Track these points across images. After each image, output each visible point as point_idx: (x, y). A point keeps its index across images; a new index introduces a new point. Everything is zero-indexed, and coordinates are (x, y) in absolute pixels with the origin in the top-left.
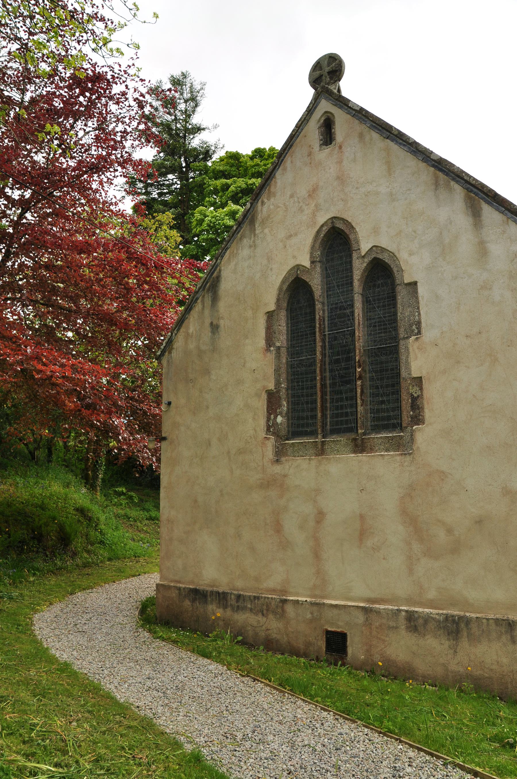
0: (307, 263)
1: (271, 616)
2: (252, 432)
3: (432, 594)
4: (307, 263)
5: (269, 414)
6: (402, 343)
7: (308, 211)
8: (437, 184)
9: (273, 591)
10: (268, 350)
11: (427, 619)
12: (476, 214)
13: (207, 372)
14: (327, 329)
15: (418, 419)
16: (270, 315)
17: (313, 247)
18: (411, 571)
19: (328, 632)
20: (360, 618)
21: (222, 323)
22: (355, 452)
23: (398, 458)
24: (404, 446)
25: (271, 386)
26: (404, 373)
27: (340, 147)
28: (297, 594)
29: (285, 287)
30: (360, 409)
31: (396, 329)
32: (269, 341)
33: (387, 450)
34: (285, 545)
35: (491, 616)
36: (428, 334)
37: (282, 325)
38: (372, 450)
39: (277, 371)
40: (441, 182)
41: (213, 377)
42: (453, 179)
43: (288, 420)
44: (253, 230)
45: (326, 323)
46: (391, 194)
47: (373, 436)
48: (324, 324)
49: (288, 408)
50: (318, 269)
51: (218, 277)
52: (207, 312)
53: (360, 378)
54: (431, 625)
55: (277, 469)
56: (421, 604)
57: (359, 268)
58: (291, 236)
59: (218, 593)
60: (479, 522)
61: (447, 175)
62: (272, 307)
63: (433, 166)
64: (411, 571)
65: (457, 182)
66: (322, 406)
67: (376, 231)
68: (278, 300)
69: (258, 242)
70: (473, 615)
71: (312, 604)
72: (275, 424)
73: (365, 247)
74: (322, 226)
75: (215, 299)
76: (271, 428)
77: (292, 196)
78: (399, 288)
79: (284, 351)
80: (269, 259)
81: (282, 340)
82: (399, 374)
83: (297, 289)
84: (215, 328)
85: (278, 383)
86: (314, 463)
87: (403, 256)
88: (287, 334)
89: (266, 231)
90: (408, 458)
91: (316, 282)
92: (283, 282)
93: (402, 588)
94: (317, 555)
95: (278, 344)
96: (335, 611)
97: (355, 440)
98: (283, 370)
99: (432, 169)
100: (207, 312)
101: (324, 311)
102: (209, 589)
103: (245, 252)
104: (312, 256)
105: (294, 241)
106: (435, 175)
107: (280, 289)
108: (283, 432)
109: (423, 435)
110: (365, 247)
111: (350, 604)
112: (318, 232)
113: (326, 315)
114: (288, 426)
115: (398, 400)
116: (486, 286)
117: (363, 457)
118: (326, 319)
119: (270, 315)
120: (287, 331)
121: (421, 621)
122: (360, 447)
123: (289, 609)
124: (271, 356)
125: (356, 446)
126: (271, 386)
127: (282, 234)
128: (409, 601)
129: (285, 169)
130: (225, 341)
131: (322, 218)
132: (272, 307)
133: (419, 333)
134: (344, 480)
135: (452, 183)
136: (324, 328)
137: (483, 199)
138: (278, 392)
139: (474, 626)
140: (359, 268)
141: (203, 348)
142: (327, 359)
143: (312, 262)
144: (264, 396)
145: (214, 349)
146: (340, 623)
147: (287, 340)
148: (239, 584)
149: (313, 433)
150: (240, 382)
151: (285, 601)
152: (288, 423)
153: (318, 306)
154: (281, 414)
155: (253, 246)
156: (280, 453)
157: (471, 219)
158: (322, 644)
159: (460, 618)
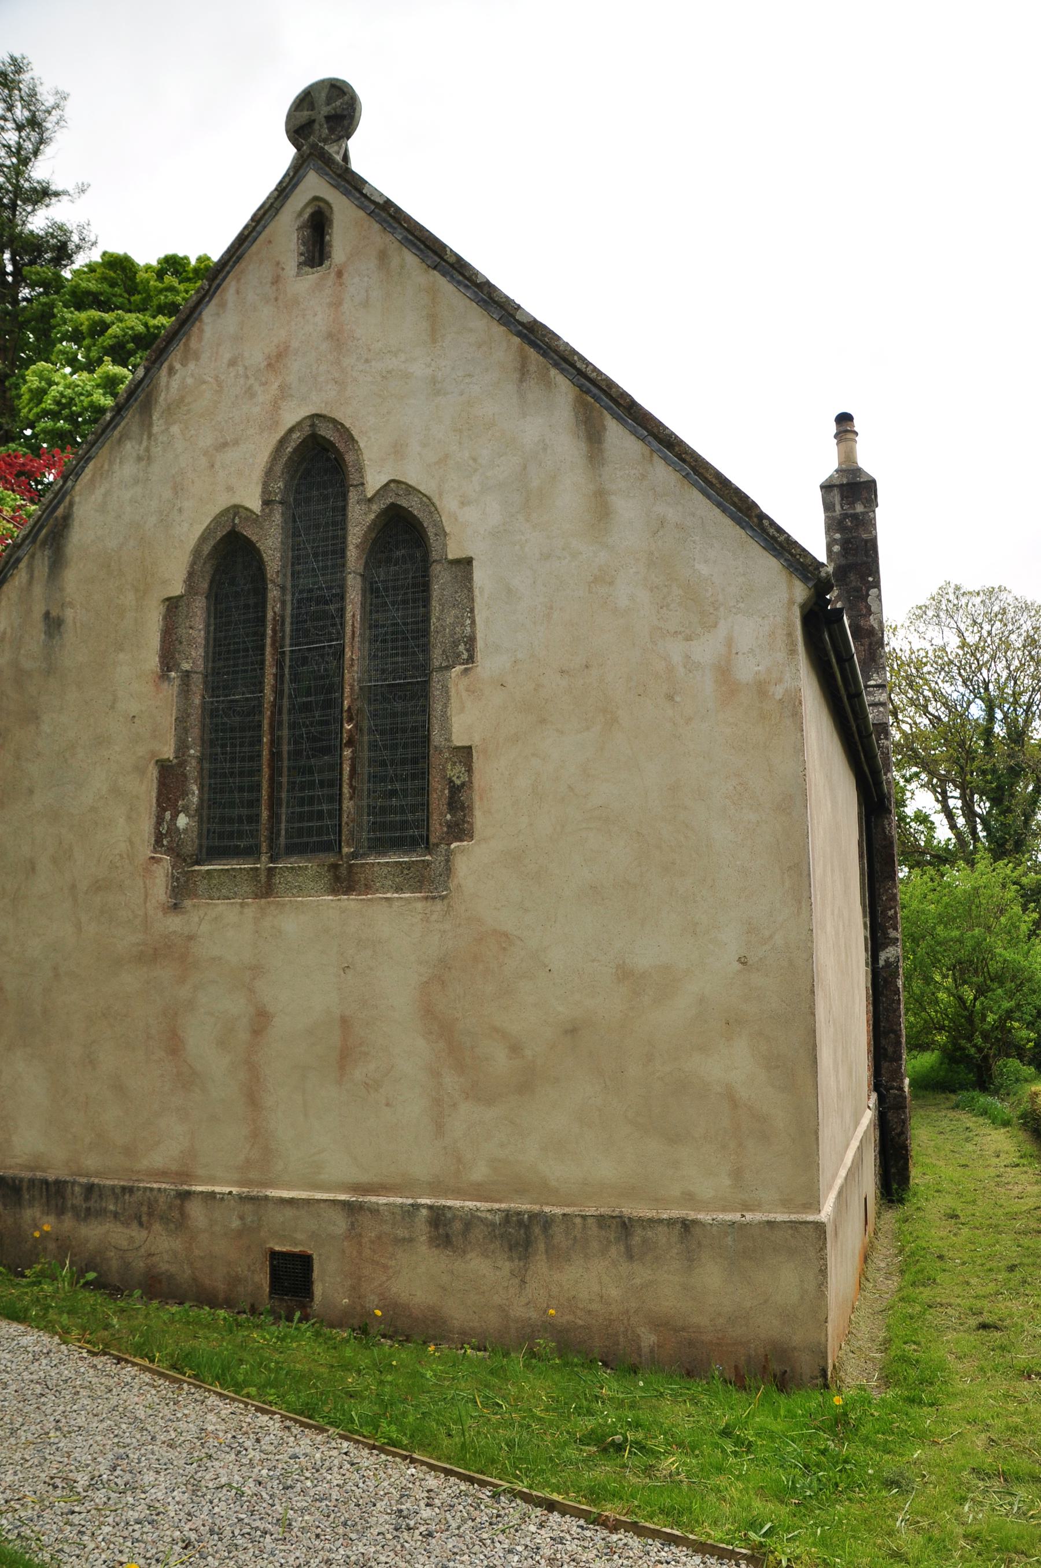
0: (255, 504)
1: (157, 1227)
2: (123, 846)
3: (479, 1173)
4: (255, 504)
5: (161, 809)
6: (436, 677)
7: (264, 397)
8: (523, 371)
9: (162, 1174)
10: (164, 676)
11: (470, 1221)
12: (593, 437)
13: (32, 716)
14: (288, 641)
15: (460, 829)
16: (172, 605)
17: (269, 472)
18: (439, 1129)
19: (274, 1255)
20: (340, 1224)
21: (69, 614)
22: (334, 891)
23: (419, 905)
24: (430, 883)
25: (168, 752)
26: (437, 738)
27: (340, 274)
28: (212, 1180)
29: (207, 549)
30: (347, 805)
31: (426, 649)
32: (168, 659)
33: (399, 889)
34: (188, 1079)
35: (591, 1211)
36: (489, 663)
37: (196, 628)
38: (368, 888)
39: (181, 721)
40: (533, 368)
41: (46, 728)
42: (556, 365)
43: (200, 822)
44: (147, 424)
45: (288, 629)
46: (434, 381)
47: (370, 860)
48: (283, 631)
49: (201, 799)
50: (277, 517)
51: (67, 518)
52: (38, 589)
53: (350, 743)
54: (478, 1233)
55: (175, 923)
56: (459, 1193)
57: (359, 521)
58: (225, 445)
59: (45, 1182)
60: (572, 1031)
61: (545, 355)
62: (177, 589)
63: (519, 334)
64: (439, 1129)
65: (562, 371)
66: (271, 797)
67: (398, 451)
68: (191, 574)
69: (156, 450)
70: (558, 1211)
71: (242, 1199)
72: (173, 830)
73: (374, 480)
74: (291, 430)
75: (57, 563)
76: (164, 838)
77: (232, 363)
78: (436, 569)
79: (197, 680)
80: (178, 489)
81: (194, 657)
82: (427, 740)
83: (229, 554)
84: (53, 624)
85: (182, 747)
86: (250, 912)
87: (448, 505)
88: (206, 646)
89: (175, 429)
90: (439, 906)
91: (271, 544)
92: (203, 539)
93: (422, 1161)
94: (253, 1099)
95: (186, 666)
96: (289, 1212)
97: (335, 867)
98: (195, 719)
99: (517, 340)
100: (38, 589)
101: (283, 603)
102: (26, 1175)
103: (126, 470)
104: (265, 490)
105: (230, 455)
106: (522, 350)
107: (197, 552)
108: (190, 848)
109: (471, 862)
110: (374, 480)
111: (319, 1196)
112: (283, 441)
113: (288, 611)
114: (200, 836)
115: (424, 791)
116: (603, 578)
117: (350, 902)
118: (288, 620)
119: (172, 605)
120: (207, 639)
121: (458, 1226)
122: (344, 881)
123: (196, 1210)
124: (171, 690)
125: (337, 879)
126: (168, 752)
127: (207, 440)
128: (436, 1187)
129: (223, 305)
130: (75, 651)
131: (292, 415)
132: (177, 589)
133: (471, 659)
134: (311, 947)
135: (553, 372)
136: (283, 638)
137: (608, 409)
138: (182, 764)
139: (558, 1232)
140: (359, 521)
141: (27, 664)
142: (286, 702)
143: (266, 503)
144: (153, 772)
145: (50, 669)
146: (300, 1236)
147: (206, 658)
148: (91, 1162)
149: (251, 852)
150: (101, 741)
151: (188, 1195)
152: (200, 830)
153: (273, 593)
154: (186, 810)
155: (146, 458)
156: (181, 892)
157: (583, 445)
158: (263, 1279)
159: (533, 1216)
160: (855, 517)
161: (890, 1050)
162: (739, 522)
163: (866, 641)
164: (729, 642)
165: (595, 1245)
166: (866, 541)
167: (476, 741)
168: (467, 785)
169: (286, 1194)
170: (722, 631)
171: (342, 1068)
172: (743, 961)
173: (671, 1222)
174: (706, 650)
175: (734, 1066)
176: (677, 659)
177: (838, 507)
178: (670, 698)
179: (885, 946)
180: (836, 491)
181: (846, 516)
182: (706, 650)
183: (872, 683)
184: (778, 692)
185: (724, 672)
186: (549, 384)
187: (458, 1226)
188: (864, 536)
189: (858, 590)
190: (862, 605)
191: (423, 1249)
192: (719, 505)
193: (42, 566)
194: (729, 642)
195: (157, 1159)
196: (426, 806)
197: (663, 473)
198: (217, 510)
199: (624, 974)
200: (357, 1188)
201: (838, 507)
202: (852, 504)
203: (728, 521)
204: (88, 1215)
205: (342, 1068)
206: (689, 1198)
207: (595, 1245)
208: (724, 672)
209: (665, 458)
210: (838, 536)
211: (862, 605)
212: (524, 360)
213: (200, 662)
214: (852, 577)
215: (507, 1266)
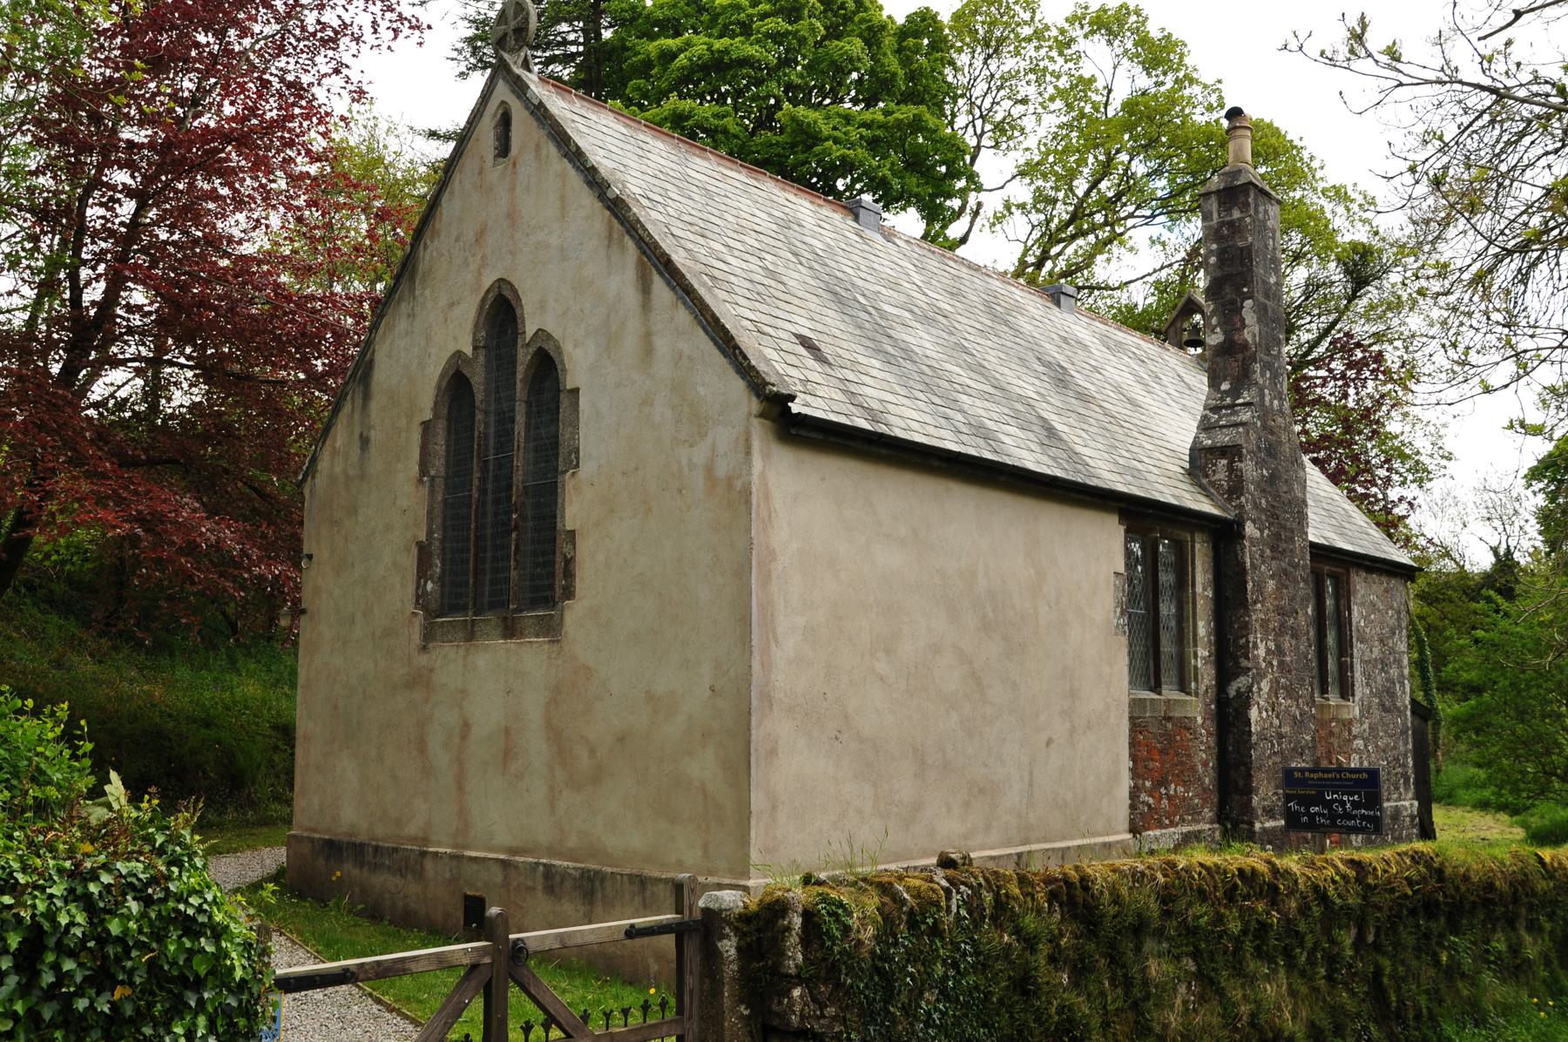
0: (468, 350)
1: (410, 877)
2: (399, 604)
3: (572, 841)
4: (468, 350)
5: (419, 578)
6: (560, 478)
7: (474, 264)
8: (610, 238)
9: (414, 839)
10: (420, 481)
11: (565, 874)
12: (645, 288)
13: (353, 510)
14: (492, 451)
15: (569, 593)
16: (426, 426)
17: (476, 325)
18: (552, 806)
19: (467, 897)
20: (497, 876)
21: (373, 434)
22: (505, 637)
23: (546, 647)
24: (551, 629)
25: (423, 537)
26: (559, 526)
27: (514, 164)
28: (439, 844)
29: (444, 384)
30: (514, 574)
31: (556, 456)
32: (424, 470)
33: (537, 636)
34: (428, 772)
35: (627, 871)
36: (587, 468)
37: (440, 445)
38: (522, 635)
39: (430, 513)
40: (615, 236)
41: (361, 519)
42: (628, 232)
43: (443, 586)
44: (412, 290)
45: (492, 442)
46: (562, 249)
47: (525, 614)
48: (487, 445)
49: (443, 571)
50: (481, 359)
51: (371, 361)
52: (357, 416)
53: (516, 528)
54: (568, 884)
55: (423, 660)
56: (562, 856)
57: (524, 357)
58: (452, 304)
59: (354, 844)
60: (621, 739)
61: (622, 224)
62: (428, 415)
63: (609, 208)
64: (552, 806)
65: (632, 236)
66: (475, 568)
67: (542, 306)
68: (436, 403)
69: (417, 309)
70: (609, 870)
71: (453, 857)
72: (425, 592)
73: (530, 330)
74: (488, 291)
75: (367, 396)
76: (420, 598)
77: (457, 240)
78: (562, 395)
79: (439, 482)
80: (428, 339)
81: (438, 466)
82: (553, 527)
83: (456, 384)
84: (365, 441)
85: (430, 533)
86: (461, 651)
87: (567, 347)
88: (448, 456)
89: (427, 292)
90: (556, 648)
91: (478, 378)
92: (442, 376)
93: (543, 833)
94: (460, 787)
95: (432, 473)
96: (475, 867)
97: (505, 619)
98: (438, 508)
99: (607, 213)
100: (357, 416)
101: (487, 424)
102: (346, 839)
103: (402, 325)
104: (475, 340)
105: (457, 311)
106: (610, 221)
107: (439, 387)
108: (434, 606)
109: (574, 613)
110: (530, 330)
111: (491, 855)
112: (483, 300)
113: (492, 430)
114: (442, 596)
115: (553, 563)
116: (647, 401)
117: (511, 644)
118: (492, 436)
119: (426, 426)
120: (448, 452)
121: (558, 879)
122: (510, 630)
123: (429, 865)
124: (425, 491)
125: (506, 628)
126: (423, 537)
127: (443, 302)
128: (551, 852)
129: (452, 193)
130: (376, 465)
131: (487, 282)
132: (428, 415)
133: (577, 466)
134: (494, 675)
135: (627, 238)
136: (487, 449)
137: (655, 266)
138: (430, 544)
139: (608, 884)
140: (524, 357)
141: (351, 472)
142: (489, 497)
143: (475, 348)
144: (415, 551)
145: (363, 476)
146: (479, 884)
147: (447, 465)
148: (380, 830)
149: (462, 609)
150: (388, 528)
151: (424, 854)
152: (442, 593)
153: (479, 416)
154: (431, 578)
155: (412, 316)
156: (429, 635)
157: (640, 296)
158: (460, 915)
159: (597, 873)
160: (1231, 224)
161: (1241, 783)
162: (723, 352)
163: (1240, 356)
164: (713, 447)
165: (628, 896)
166: (1242, 249)
167: (577, 527)
168: (573, 558)
169: (474, 854)
170: (709, 440)
171: (505, 764)
172: (712, 689)
173: (666, 881)
174: (700, 455)
175: (704, 767)
176: (684, 462)
177: (1215, 215)
178: (680, 491)
179: (1236, 676)
180: (1213, 198)
181: (1222, 224)
182: (700, 455)
183: (1240, 401)
184: (738, 484)
185: (709, 470)
186: (623, 248)
187: (558, 879)
188: (1240, 244)
189: (1232, 302)
190: (1236, 319)
191: (540, 894)
192: (713, 339)
193: (359, 401)
194: (713, 447)
195: (412, 829)
196: (552, 575)
197: (683, 316)
198: (449, 354)
199: (650, 698)
200: (513, 851)
201: (1215, 215)
202: (1229, 210)
203: (717, 352)
204: (375, 868)
205: (505, 764)
206: (680, 866)
207: (628, 896)
208: (709, 470)
209: (685, 303)
210: (1214, 246)
211: (1236, 319)
212: (611, 228)
213: (442, 469)
214: (1228, 289)
215: (582, 909)
